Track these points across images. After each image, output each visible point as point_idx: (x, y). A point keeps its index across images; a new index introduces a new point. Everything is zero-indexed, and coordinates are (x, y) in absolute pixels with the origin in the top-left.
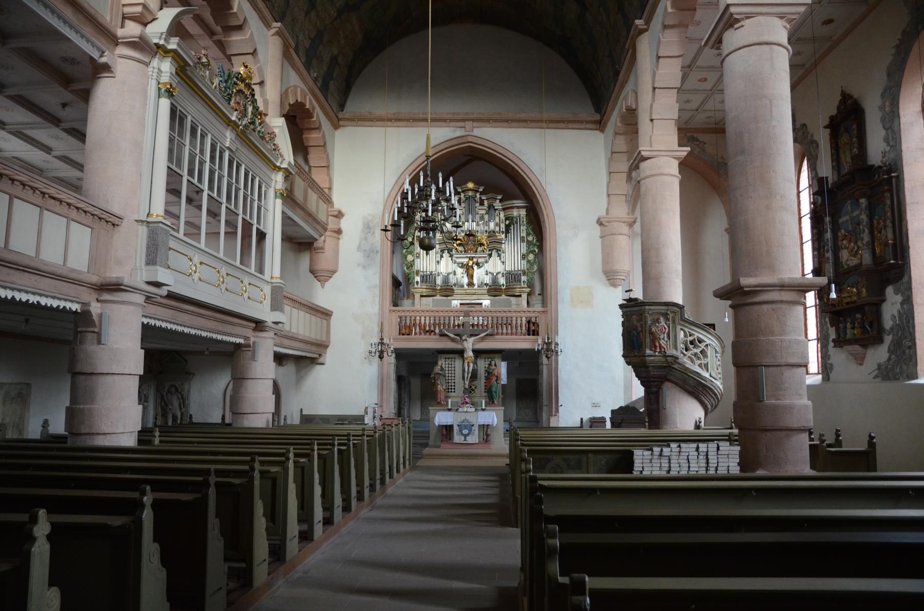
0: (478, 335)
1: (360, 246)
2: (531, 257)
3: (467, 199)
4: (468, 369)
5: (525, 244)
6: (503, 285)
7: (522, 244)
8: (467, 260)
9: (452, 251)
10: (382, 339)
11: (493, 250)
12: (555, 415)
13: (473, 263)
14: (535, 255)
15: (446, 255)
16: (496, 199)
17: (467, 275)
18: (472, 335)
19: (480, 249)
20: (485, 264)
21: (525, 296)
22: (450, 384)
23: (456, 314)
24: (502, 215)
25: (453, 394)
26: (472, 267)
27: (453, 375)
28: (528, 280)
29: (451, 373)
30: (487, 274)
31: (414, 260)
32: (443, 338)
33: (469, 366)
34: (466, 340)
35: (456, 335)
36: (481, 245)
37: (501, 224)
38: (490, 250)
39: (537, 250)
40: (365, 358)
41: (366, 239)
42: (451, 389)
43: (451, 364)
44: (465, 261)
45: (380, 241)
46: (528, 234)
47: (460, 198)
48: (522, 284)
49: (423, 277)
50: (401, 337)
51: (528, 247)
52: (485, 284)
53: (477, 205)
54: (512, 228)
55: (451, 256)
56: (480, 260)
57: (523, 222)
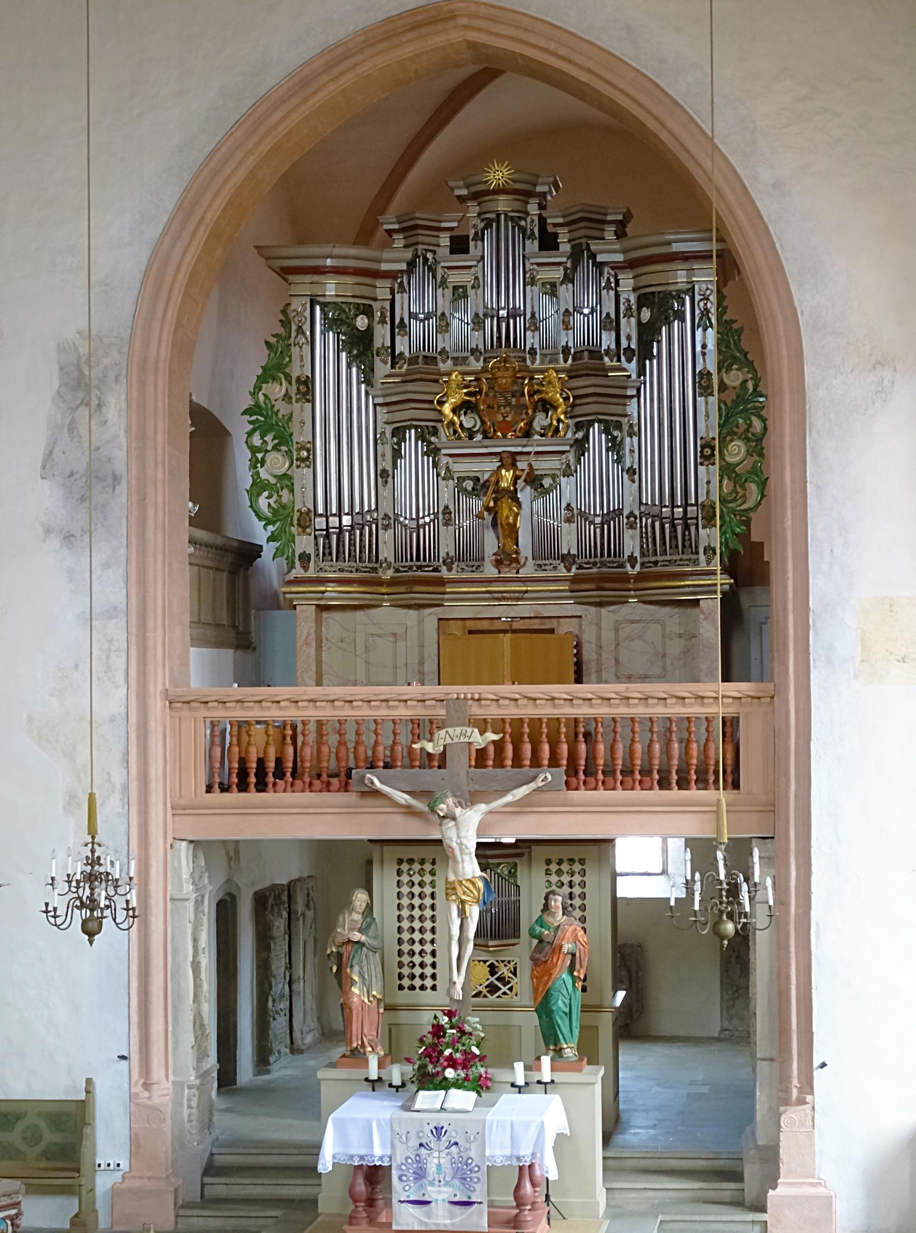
1: (49, 455)
4: (462, 927)
5: (713, 400)
6: (632, 560)
8: (494, 464)
9: (435, 432)
10: (94, 861)
11: (591, 423)
12: (801, 1102)
13: (516, 478)
15: (411, 445)
17: (494, 524)
19: (540, 421)
20: (564, 480)
21: (712, 605)
23: (419, 712)
24: (627, 283)
25: (428, 997)
26: (513, 496)
27: (428, 925)
29: (422, 919)
30: (569, 520)
32: (370, 801)
36: (546, 406)
37: (623, 321)
38: (578, 426)
41: (72, 428)
42: (422, 977)
43: (421, 884)
44: (485, 468)
45: (123, 439)
48: (702, 557)
49: (328, 536)
50: (217, 797)
53: (533, 246)
55: (433, 452)
56: (543, 465)
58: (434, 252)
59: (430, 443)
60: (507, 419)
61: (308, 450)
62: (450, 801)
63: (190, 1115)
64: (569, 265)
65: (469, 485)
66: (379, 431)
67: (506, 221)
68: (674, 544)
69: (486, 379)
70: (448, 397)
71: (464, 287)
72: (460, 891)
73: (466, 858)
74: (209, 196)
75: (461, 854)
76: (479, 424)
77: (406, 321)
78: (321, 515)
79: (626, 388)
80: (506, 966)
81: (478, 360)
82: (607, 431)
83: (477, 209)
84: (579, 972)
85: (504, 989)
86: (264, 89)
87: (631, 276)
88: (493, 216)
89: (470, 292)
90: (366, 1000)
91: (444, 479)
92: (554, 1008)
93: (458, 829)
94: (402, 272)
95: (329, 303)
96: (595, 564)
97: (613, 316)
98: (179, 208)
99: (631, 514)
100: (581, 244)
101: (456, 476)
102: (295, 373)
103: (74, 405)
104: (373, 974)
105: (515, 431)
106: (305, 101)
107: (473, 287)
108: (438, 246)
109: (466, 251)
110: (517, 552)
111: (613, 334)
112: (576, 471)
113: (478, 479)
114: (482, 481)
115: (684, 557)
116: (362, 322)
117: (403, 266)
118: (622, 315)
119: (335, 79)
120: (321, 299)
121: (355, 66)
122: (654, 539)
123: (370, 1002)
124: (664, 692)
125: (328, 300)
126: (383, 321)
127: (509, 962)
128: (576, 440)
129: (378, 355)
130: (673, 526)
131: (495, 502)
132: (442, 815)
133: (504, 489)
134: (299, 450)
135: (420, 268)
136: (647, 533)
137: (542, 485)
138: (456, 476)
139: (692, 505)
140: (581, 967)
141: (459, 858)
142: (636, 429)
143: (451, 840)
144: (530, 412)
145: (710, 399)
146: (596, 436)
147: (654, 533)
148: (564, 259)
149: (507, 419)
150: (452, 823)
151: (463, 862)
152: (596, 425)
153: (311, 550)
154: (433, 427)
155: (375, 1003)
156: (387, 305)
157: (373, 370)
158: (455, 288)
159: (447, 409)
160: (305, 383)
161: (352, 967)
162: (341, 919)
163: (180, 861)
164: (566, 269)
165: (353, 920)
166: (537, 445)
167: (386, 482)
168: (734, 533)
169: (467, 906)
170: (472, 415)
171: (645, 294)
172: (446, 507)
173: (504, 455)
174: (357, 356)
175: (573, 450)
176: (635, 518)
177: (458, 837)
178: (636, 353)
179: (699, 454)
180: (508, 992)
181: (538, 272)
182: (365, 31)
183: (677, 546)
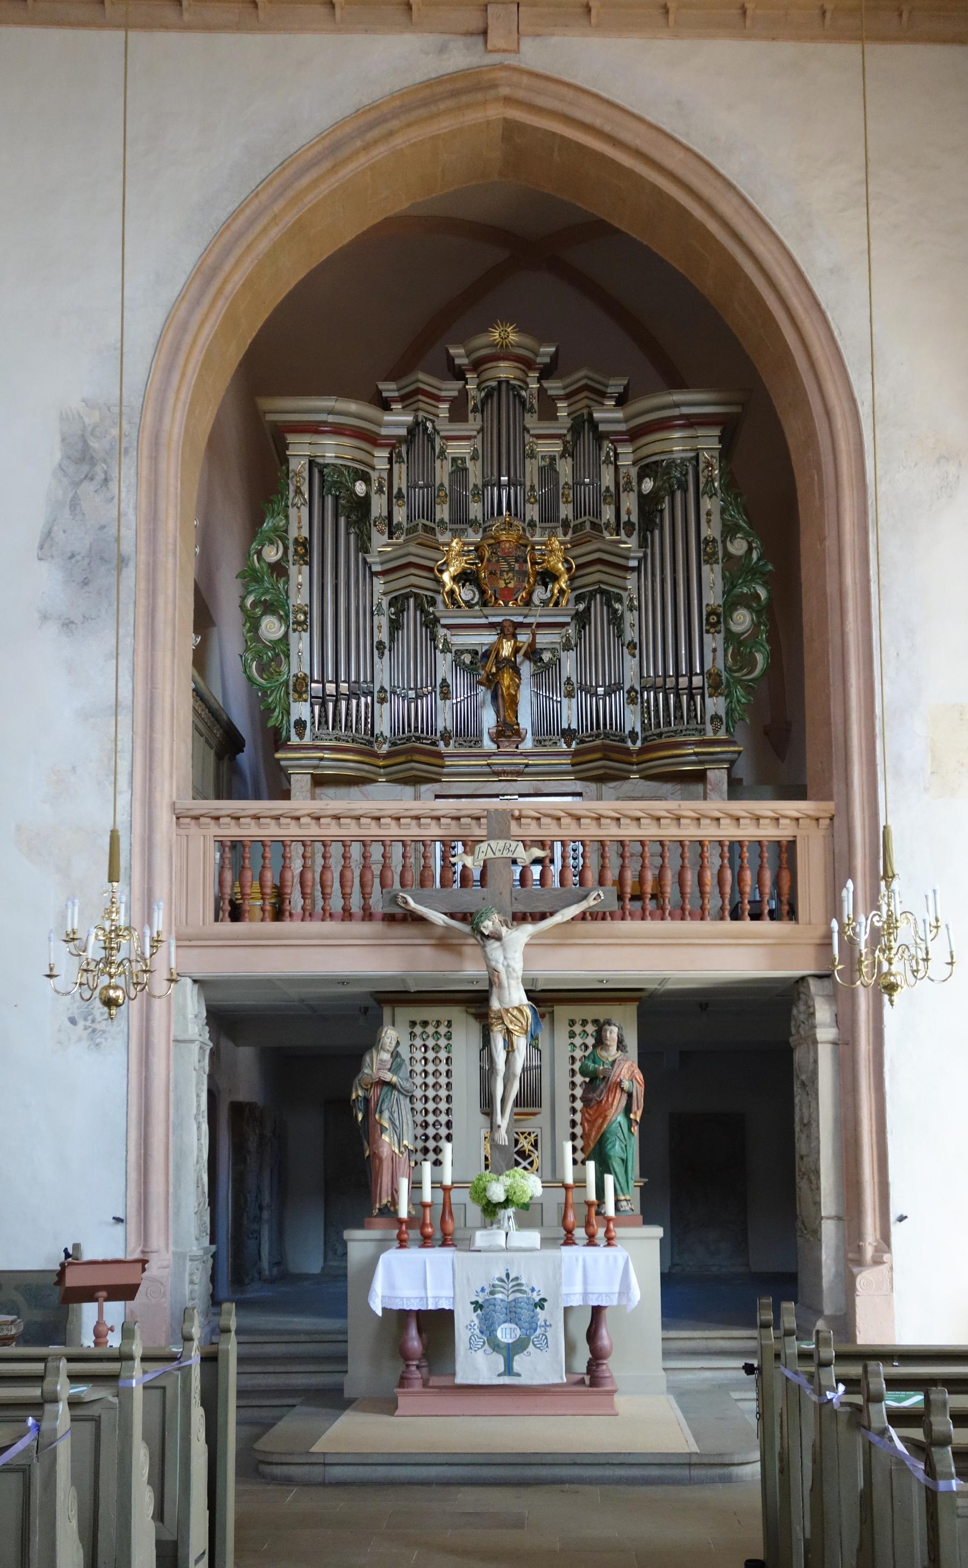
0: (543, 916)
2: (742, 620)
3: (489, 396)
5: (718, 568)
7: (706, 568)
9: (433, 602)
11: (592, 595)
13: (516, 650)
14: (758, 613)
16: (603, 395)
18: (520, 918)
19: (540, 594)
20: (563, 655)
22: (431, 1131)
23: (454, 830)
28: (729, 712)
31: (286, 635)
32: (399, 930)
33: (510, 1048)
34: (498, 938)
35: (452, 916)
36: (547, 577)
37: (623, 496)
38: (578, 599)
39: (763, 594)
40: (73, 1021)
46: (729, 531)
47: (464, 393)
48: (709, 727)
51: (730, 583)
52: (563, 731)
54: (666, 505)
56: (545, 639)
57: (710, 480)
58: (433, 422)
59: (428, 613)
60: (509, 585)
61: (305, 614)
62: (496, 917)
63: (191, 1292)
64: (569, 438)
65: (467, 658)
66: (375, 602)
67: (508, 390)
68: (679, 714)
69: (489, 545)
70: (448, 565)
71: (463, 460)
72: (507, 1022)
73: (513, 982)
74: (232, 260)
75: (508, 978)
76: (477, 596)
77: (404, 491)
78: (317, 682)
79: (628, 558)
81: (476, 532)
82: (609, 606)
83: (477, 381)
84: (635, 1113)
85: (525, 1164)
86: (293, 147)
87: (630, 450)
88: (494, 384)
89: (469, 464)
90: (397, 1151)
91: (442, 651)
92: (612, 1153)
93: (504, 950)
94: (400, 439)
95: (328, 464)
96: (598, 736)
97: (612, 489)
98: (198, 269)
99: (632, 689)
100: (583, 414)
101: (454, 649)
102: (293, 533)
103: (77, 480)
104: (405, 1120)
105: (516, 600)
106: (334, 169)
107: (473, 458)
108: (437, 416)
109: (466, 420)
110: (518, 724)
111: (613, 507)
112: (576, 646)
113: (476, 653)
114: (480, 654)
115: (690, 727)
116: (360, 488)
117: (403, 432)
118: (621, 489)
119: (366, 148)
120: (320, 461)
121: (391, 134)
122: (657, 711)
123: (402, 1153)
124: (718, 810)
125: (327, 461)
126: (380, 490)
128: (577, 612)
129: (375, 526)
130: (678, 696)
131: (498, 669)
132: (486, 933)
133: (505, 658)
134: (296, 613)
135: (420, 438)
136: (648, 707)
137: (541, 659)
138: (454, 649)
139: (697, 674)
140: (638, 1108)
141: (505, 983)
142: (636, 603)
143: (497, 962)
144: (532, 580)
145: (715, 566)
146: (598, 610)
147: (657, 705)
148: (565, 431)
149: (509, 585)
150: (497, 944)
151: (509, 987)
152: (598, 596)
153: (306, 716)
154: (432, 597)
155: (406, 1154)
156: (385, 475)
157: (370, 539)
158: (454, 460)
159: (446, 577)
160: (303, 545)
161: (381, 1112)
162: (368, 1059)
163: (185, 997)
164: (565, 443)
165: (382, 1061)
166: (540, 616)
167: (383, 654)
168: (739, 701)
169: (515, 1038)
170: (471, 587)
171: (647, 465)
172: (444, 680)
173: (505, 624)
174: (356, 522)
175: (573, 625)
176: (636, 692)
177: (505, 958)
178: (637, 527)
179: (704, 622)
180: (528, 1167)
181: (537, 444)
182: (403, 93)
183: (682, 717)
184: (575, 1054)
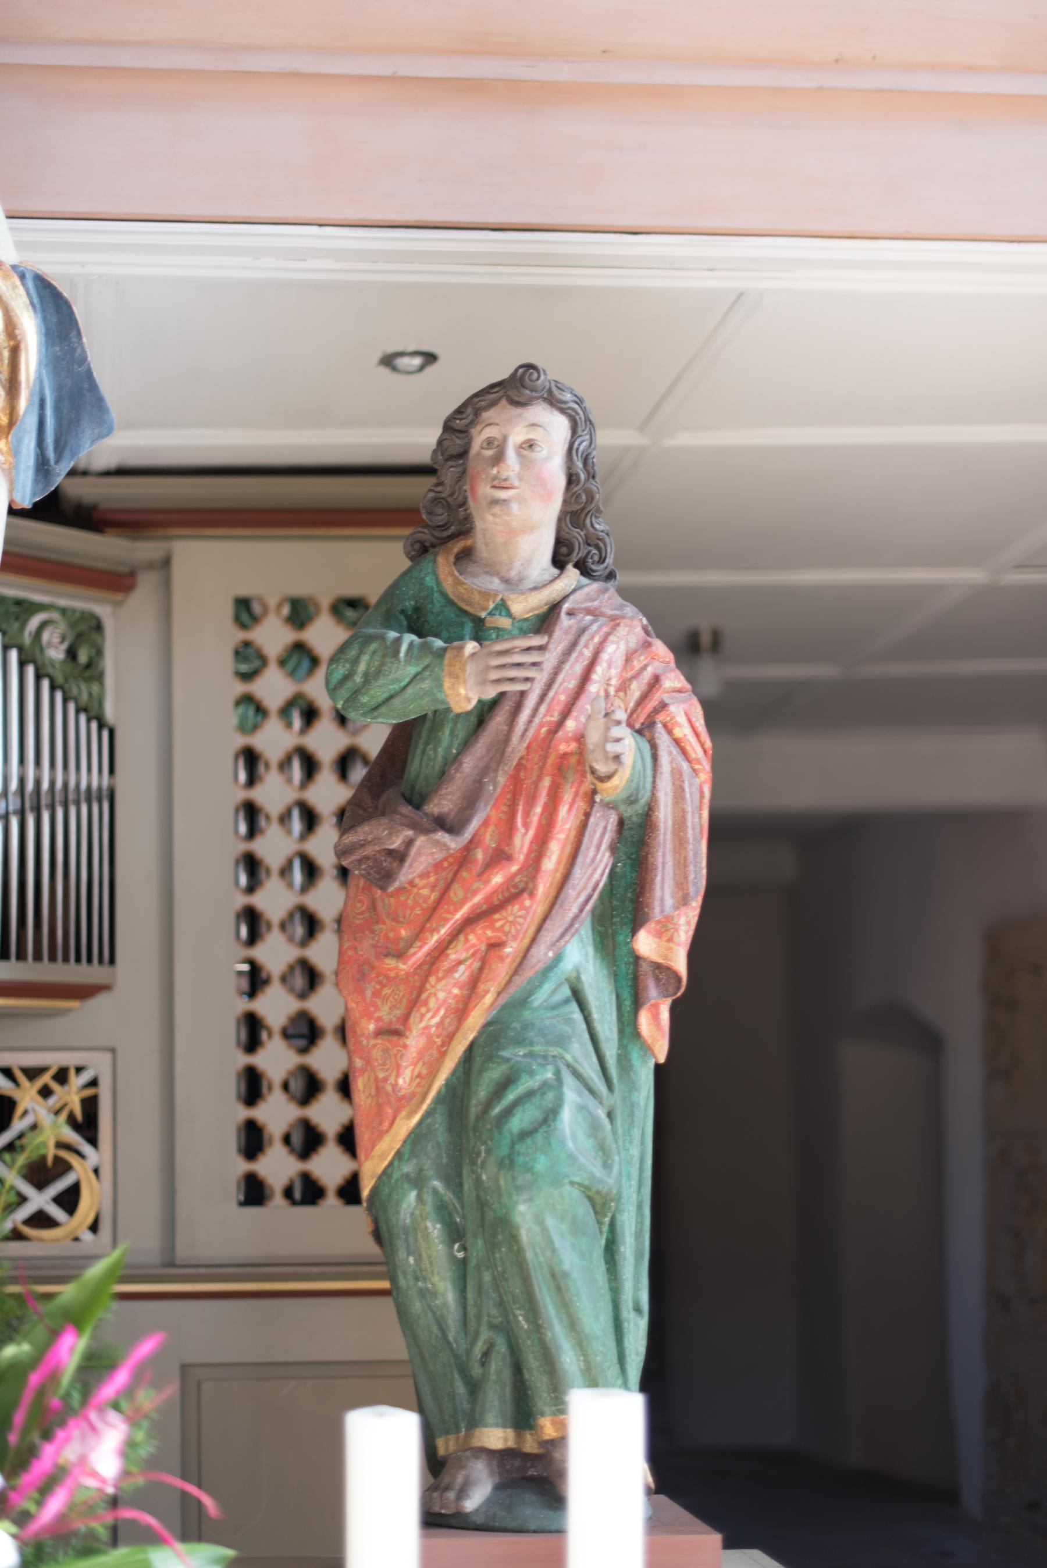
80: (45, 1092)
84: (665, 931)
85: (41, 1200)
127: (62, 1076)
140: (684, 901)
180: (56, 1212)
184: (259, 741)
